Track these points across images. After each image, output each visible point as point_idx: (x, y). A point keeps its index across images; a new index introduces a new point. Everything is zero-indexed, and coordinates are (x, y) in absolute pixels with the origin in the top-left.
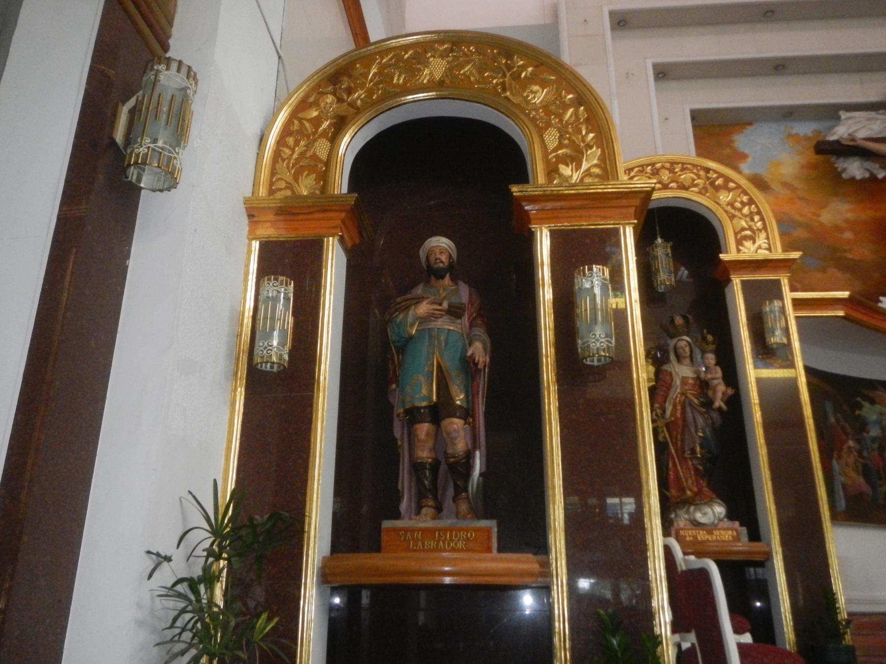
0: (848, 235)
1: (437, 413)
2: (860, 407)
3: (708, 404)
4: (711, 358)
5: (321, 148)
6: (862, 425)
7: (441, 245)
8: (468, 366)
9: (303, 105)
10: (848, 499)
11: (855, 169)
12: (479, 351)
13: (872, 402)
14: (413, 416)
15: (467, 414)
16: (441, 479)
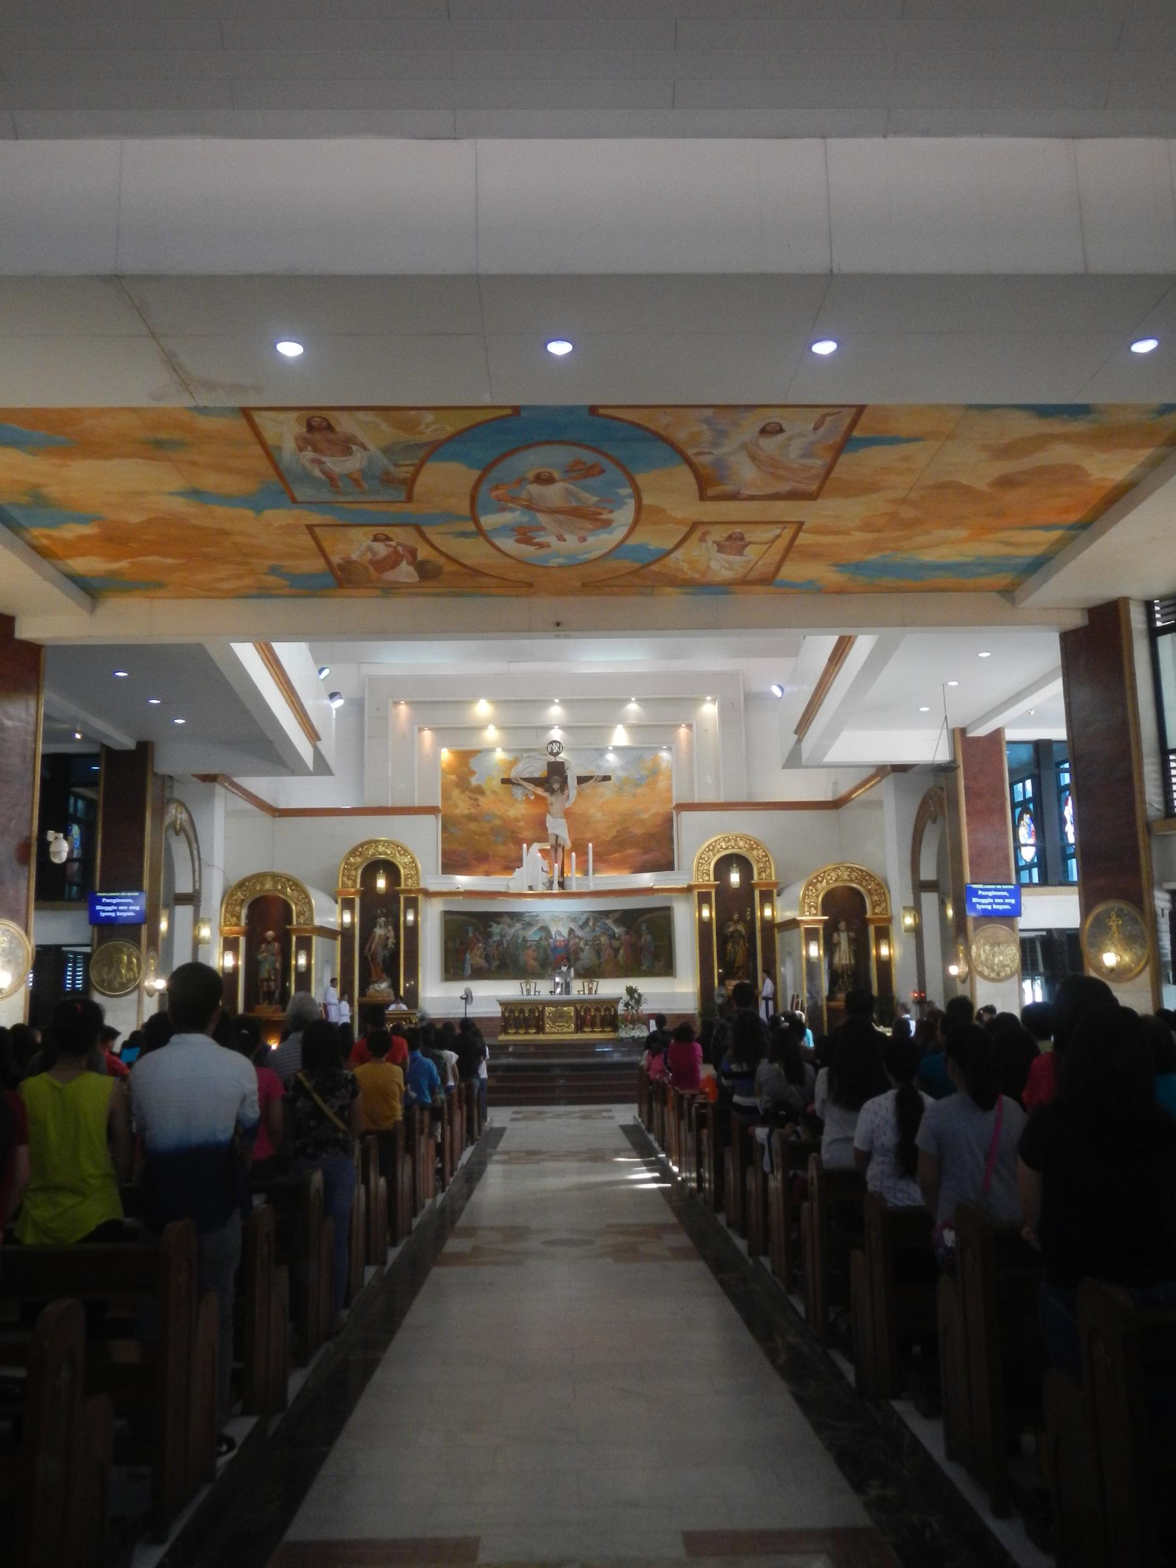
0: (522, 824)
1: (268, 980)
2: (490, 926)
3: (386, 945)
4: (390, 928)
5: (238, 908)
6: (490, 935)
7: (270, 933)
8: (275, 969)
9: (232, 895)
10: (473, 971)
11: (518, 793)
12: (278, 965)
13: (498, 923)
14: (263, 980)
15: (275, 981)
16: (269, 996)
